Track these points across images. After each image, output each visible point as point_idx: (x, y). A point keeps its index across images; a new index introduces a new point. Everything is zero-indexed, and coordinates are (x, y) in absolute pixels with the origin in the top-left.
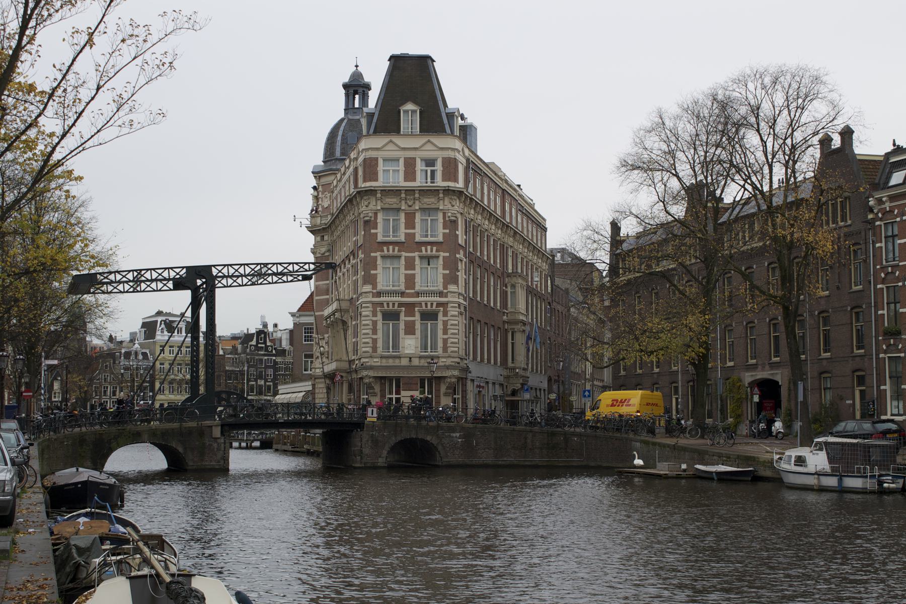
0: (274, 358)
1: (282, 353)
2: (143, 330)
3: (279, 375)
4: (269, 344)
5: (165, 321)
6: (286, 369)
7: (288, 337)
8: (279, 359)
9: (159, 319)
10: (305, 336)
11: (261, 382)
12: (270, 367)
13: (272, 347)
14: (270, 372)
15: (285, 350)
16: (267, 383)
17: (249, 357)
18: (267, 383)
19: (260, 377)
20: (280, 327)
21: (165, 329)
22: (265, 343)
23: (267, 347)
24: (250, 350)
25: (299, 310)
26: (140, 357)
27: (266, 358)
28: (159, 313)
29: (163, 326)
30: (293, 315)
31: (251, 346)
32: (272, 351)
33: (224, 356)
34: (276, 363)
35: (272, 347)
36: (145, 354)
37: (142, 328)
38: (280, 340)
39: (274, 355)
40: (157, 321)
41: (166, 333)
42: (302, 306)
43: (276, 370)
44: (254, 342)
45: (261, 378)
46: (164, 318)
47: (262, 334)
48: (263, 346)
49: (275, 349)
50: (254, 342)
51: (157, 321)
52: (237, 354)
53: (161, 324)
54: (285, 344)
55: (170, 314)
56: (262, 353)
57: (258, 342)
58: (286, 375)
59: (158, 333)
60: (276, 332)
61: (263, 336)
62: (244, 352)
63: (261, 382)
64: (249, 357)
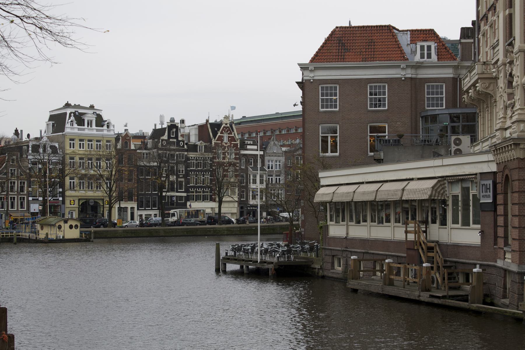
0: (186, 153)
1: (194, 148)
2: (51, 123)
3: (191, 171)
4: (180, 138)
5: (74, 113)
6: (197, 165)
7: (197, 133)
8: (192, 155)
9: (68, 111)
10: (322, 100)
11: (173, 178)
12: (181, 163)
13: (183, 141)
14: (182, 168)
15: (197, 145)
16: (179, 180)
17: (160, 152)
18: (179, 180)
19: (171, 171)
20: (187, 124)
21: (75, 122)
22: (177, 137)
23: (178, 141)
24: (162, 145)
25: (313, 60)
26: (49, 150)
27: (177, 153)
28: (68, 105)
29: (72, 118)
30: (303, 68)
31: (162, 140)
32: (183, 146)
33: (135, 150)
34: (188, 159)
35: (183, 141)
36: (53, 148)
37: (49, 120)
38: (189, 136)
39: (187, 151)
40: (65, 114)
41: (75, 125)
42: (316, 55)
43: (187, 166)
44: (165, 137)
45: (173, 174)
46: (73, 110)
47: (173, 127)
48: (175, 140)
49: (186, 144)
50: (165, 137)
51: (65, 114)
52: (146, 149)
53: (70, 116)
54: (193, 139)
55: (79, 107)
56: (175, 148)
57: (169, 137)
58: (198, 171)
59: (68, 125)
60: (183, 128)
61: (174, 130)
62: (155, 146)
63: (173, 178)
64: (160, 152)
